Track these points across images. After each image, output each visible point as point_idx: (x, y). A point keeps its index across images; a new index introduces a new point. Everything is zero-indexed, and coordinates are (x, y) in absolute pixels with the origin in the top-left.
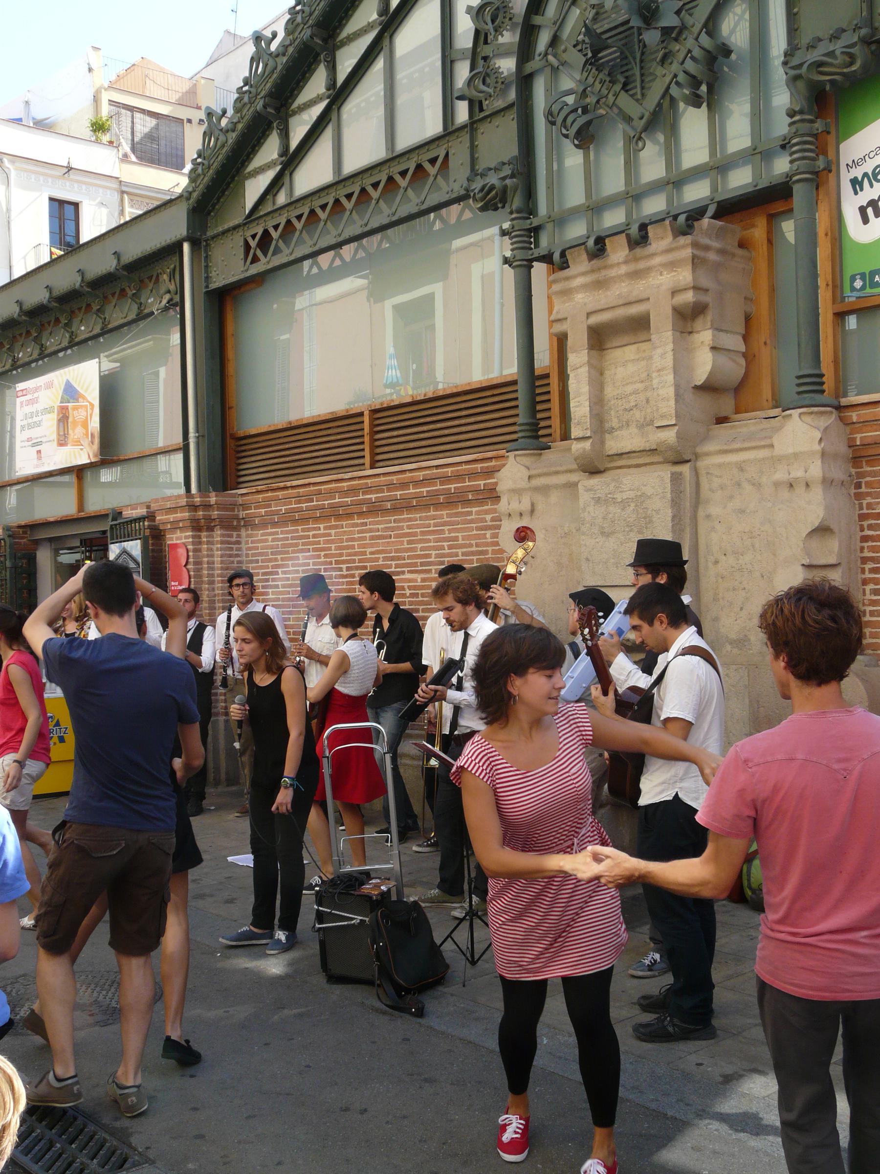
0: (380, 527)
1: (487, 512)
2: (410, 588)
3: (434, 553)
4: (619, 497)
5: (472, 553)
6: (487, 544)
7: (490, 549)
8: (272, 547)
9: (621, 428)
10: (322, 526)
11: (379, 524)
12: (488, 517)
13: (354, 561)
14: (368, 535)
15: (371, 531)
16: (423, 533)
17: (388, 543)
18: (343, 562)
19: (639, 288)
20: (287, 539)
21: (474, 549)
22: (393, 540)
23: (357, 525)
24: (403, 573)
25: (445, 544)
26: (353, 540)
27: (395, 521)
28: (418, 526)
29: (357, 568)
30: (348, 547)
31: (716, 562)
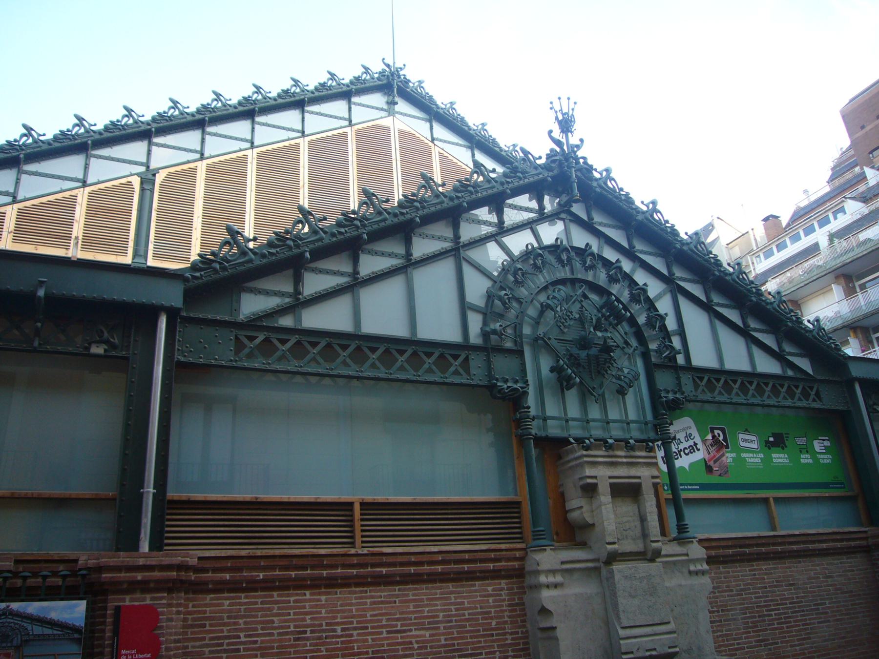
0: (383, 594)
1: (489, 585)
2: (417, 642)
3: (441, 614)
4: (638, 576)
5: (478, 613)
6: (491, 607)
7: (493, 610)
8: (230, 611)
9: (623, 539)
10: (308, 593)
11: (383, 593)
12: (490, 589)
13: (352, 623)
14: (369, 601)
15: (372, 597)
16: (428, 599)
17: (393, 607)
18: (338, 624)
19: (633, 472)
20: (256, 603)
21: (479, 610)
22: (397, 604)
23: (355, 593)
24: (411, 630)
25: (452, 607)
26: (351, 604)
27: (399, 590)
28: (425, 594)
29: (355, 629)
30: (343, 611)
31: (672, 610)
